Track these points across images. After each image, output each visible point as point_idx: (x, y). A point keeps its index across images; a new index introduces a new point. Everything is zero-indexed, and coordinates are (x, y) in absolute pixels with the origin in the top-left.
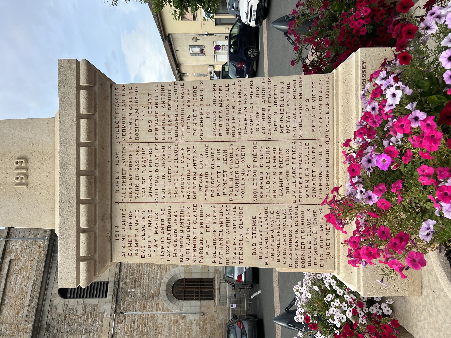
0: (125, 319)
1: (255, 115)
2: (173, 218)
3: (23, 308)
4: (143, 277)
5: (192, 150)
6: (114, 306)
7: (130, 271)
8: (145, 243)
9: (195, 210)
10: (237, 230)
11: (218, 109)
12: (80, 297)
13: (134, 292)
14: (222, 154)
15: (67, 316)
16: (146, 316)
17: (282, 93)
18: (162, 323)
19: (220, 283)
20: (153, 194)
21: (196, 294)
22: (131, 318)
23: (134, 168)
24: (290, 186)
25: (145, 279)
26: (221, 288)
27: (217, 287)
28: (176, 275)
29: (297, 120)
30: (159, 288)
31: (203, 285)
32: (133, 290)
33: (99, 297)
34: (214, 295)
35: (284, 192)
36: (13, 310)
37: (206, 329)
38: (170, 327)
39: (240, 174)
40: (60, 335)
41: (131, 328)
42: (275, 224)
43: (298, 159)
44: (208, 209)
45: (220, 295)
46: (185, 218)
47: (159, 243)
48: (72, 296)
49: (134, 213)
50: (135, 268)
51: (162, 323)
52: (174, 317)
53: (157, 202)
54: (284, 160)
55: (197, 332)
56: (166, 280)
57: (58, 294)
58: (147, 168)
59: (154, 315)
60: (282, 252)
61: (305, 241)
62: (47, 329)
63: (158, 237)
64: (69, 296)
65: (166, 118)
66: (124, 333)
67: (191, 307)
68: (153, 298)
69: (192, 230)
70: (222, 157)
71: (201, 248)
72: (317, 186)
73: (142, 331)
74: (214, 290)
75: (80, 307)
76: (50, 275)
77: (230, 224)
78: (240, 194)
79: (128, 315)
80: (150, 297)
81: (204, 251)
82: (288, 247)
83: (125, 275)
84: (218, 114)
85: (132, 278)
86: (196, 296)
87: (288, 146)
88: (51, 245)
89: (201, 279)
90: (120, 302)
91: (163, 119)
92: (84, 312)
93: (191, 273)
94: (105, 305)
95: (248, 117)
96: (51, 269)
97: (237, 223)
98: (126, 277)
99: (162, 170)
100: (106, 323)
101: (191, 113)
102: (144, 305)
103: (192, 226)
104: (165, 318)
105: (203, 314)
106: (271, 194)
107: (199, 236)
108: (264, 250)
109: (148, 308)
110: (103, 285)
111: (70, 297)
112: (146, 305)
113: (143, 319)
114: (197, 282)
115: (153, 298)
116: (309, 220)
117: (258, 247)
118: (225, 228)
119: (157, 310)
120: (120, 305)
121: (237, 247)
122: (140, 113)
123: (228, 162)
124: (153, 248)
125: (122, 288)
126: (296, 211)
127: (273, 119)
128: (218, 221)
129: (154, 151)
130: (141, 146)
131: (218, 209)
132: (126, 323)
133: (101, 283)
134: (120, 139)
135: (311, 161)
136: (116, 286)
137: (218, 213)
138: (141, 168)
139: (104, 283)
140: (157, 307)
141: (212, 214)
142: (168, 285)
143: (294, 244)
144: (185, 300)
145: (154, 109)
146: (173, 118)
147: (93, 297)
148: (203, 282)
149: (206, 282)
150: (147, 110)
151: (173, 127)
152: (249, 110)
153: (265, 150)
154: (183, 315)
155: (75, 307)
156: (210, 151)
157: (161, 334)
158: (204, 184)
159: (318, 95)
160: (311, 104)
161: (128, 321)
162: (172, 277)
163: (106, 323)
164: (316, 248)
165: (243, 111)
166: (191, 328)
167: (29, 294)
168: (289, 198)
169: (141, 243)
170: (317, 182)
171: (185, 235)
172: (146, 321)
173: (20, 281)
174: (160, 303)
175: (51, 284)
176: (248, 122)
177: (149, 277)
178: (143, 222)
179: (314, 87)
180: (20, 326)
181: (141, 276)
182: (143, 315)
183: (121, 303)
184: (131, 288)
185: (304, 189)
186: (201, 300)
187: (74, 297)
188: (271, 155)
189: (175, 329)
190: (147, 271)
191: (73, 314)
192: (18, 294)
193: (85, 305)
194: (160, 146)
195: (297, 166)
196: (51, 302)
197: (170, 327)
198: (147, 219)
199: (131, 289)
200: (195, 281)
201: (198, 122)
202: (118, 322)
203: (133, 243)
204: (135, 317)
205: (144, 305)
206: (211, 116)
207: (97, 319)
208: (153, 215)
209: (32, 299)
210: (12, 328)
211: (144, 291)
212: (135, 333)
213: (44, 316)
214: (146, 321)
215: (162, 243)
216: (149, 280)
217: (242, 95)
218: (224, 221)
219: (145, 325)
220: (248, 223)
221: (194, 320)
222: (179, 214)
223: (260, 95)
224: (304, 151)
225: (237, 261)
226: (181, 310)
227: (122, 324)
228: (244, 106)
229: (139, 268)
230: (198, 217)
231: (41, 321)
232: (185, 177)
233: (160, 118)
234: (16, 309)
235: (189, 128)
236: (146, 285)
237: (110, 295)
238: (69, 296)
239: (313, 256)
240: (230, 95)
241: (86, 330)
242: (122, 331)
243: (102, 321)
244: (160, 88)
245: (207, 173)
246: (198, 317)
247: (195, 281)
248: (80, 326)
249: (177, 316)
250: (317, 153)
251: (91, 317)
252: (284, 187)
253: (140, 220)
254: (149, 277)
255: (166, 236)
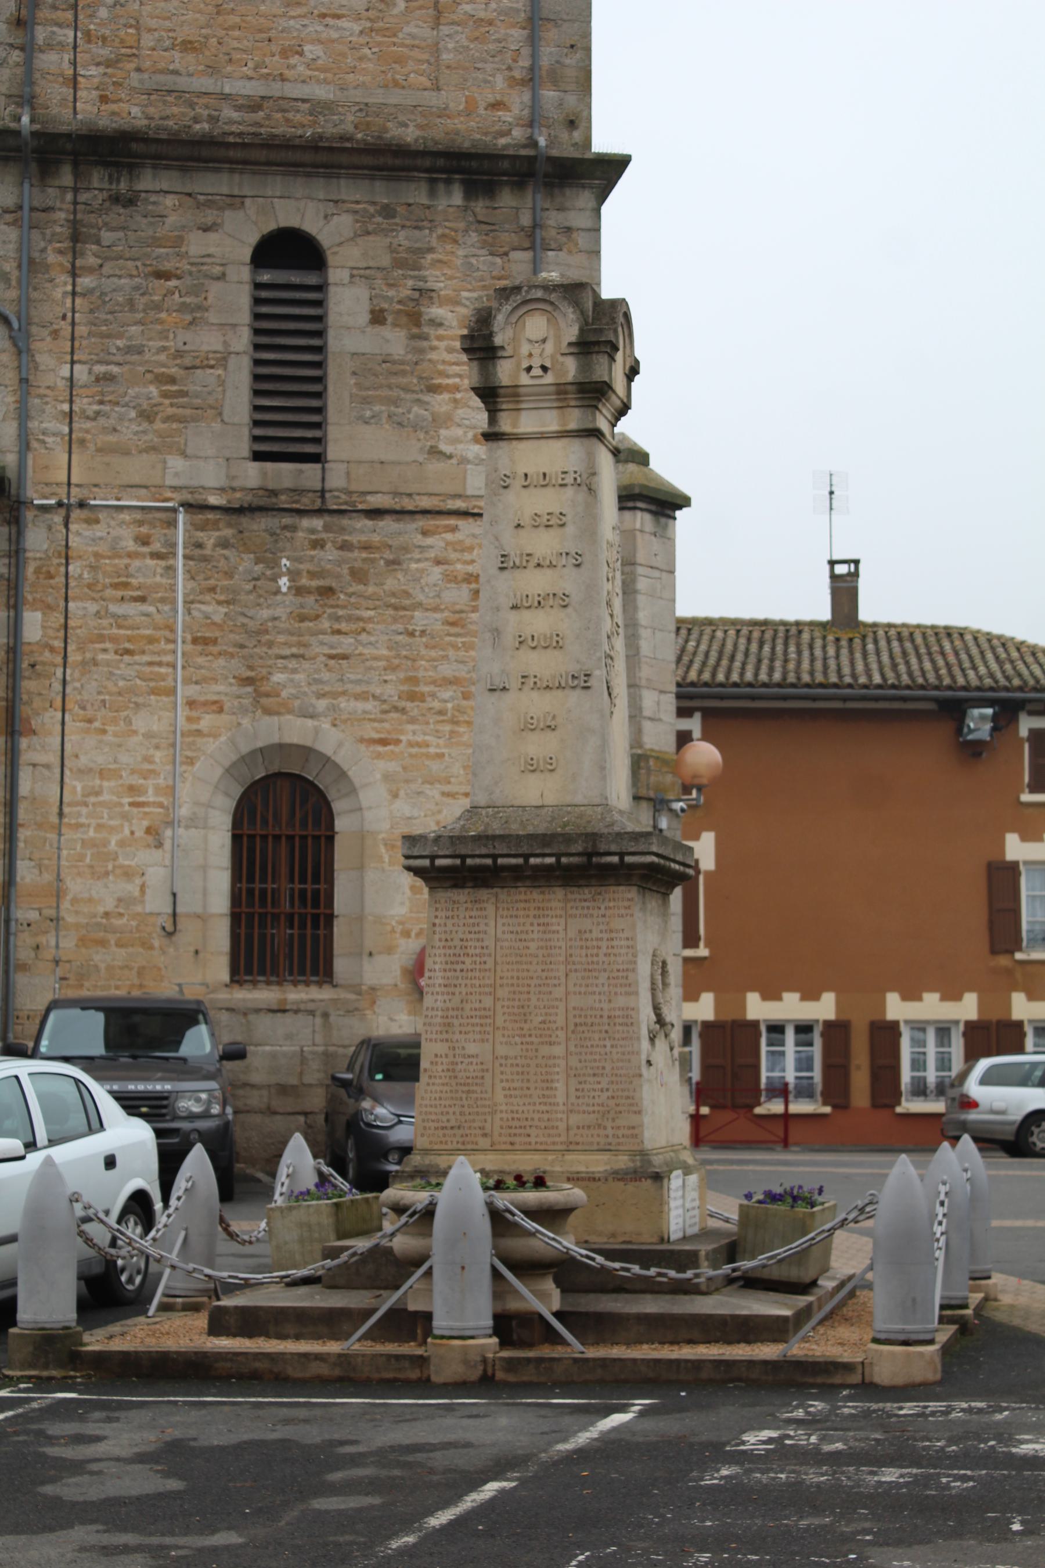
0: (156, 556)
1: (597, 1057)
2: (478, 959)
3: (212, 70)
4: (343, 626)
5: (556, 982)
6: (213, 500)
7: (373, 561)
8: (450, 927)
9: (488, 986)
10: (463, 1037)
11: (606, 1014)
12: (257, 332)
13: (278, 592)
14: (552, 1018)
15: (173, 283)
16: (165, 652)
17: (623, 1090)
18: (135, 732)
19: (312, 1013)
20: (506, 936)
21: (263, 892)
22: (159, 586)
23: (536, 912)
24: (513, 1100)
25: (336, 638)
26: (288, 1018)
27: (296, 995)
28: (353, 791)
29: (591, 1109)
30: (290, 712)
31: (303, 926)
32: (284, 582)
33: (256, 423)
34: (254, 983)
35: (507, 1092)
36: (202, 19)
37: (103, 943)
38: (116, 774)
39: (528, 1039)
40: (92, 261)
41: (116, 586)
42: (470, 1081)
43: (543, 1108)
44: (488, 1002)
45: (258, 1011)
46: (477, 974)
47: (450, 943)
48: (264, 294)
49: (484, 913)
50: (390, 584)
51: (135, 732)
52: (157, 789)
53: (497, 940)
54: (546, 1093)
55: (90, 900)
56: (330, 740)
57: (272, 226)
58: (536, 928)
59: (173, 692)
60: (438, 1088)
61: (451, 1117)
62: (115, 199)
63: (457, 942)
64: (266, 277)
65: (595, 951)
66: (97, 555)
67: (204, 871)
68: (249, 681)
69: (464, 982)
70: (549, 1018)
71: (443, 994)
72: (513, 1131)
73: (101, 639)
74: (279, 983)
75: (208, 341)
76: (364, 177)
77: (470, 1028)
78: (504, 1040)
79: (171, 570)
80: (251, 668)
81: (439, 997)
82: (443, 1095)
83: (354, 539)
84: (599, 1013)
85: (338, 576)
86: (250, 892)
87: (560, 1099)
88: (506, 165)
89: (330, 918)
90: (229, 525)
91: (593, 947)
92: (188, 361)
93: (361, 868)
94: (216, 458)
95: (594, 1050)
96: (388, 179)
97: (470, 1036)
98: (345, 546)
99: (533, 946)
100: (136, 468)
101: (601, 981)
102: (215, 641)
103: (469, 982)
104: (157, 747)
105: (170, 928)
106: (504, 1077)
107: (457, 990)
108: (440, 1068)
109: (200, 660)
110: (309, 434)
111: (258, 286)
112: (215, 649)
113: (151, 640)
114: (316, 893)
115: (249, 681)
116: (474, 1121)
117: (444, 1060)
118: (465, 1021)
119: (191, 704)
120: (215, 526)
121: (445, 1036)
122: (601, 920)
123: (542, 1026)
124: (443, 937)
125: (293, 528)
126: (484, 1106)
127: (591, 1079)
128: (473, 1013)
129: (556, 936)
130: (562, 921)
131: (487, 1013)
132: (137, 563)
133: (318, 426)
134: (570, 896)
135: (543, 1124)
136: (306, 502)
137: (483, 1013)
138: (535, 922)
139: (318, 441)
140: (205, 704)
141: (482, 1005)
142: (306, 752)
143: (447, 1103)
144: (236, 838)
145: (605, 936)
146: (595, 959)
147: (257, 393)
148: (316, 926)
149: (316, 939)
150: (603, 927)
151: (584, 959)
152: (603, 1051)
153: (557, 1069)
154: (168, 833)
155: (212, 317)
156: (556, 1003)
157: (87, 731)
158: (517, 997)
159: (620, 1133)
160: (609, 1124)
161: (146, 572)
162: (343, 775)
163: (136, 468)
164: (443, 1128)
165: (602, 1043)
166: (107, 873)
167: (276, 89)
168: (500, 1096)
169: (449, 922)
170: (518, 1131)
171: (458, 973)
172: (146, 658)
173: (335, 35)
174: (224, 717)
175: (319, 188)
176: (590, 1050)
177: (345, 657)
178: (474, 925)
179: (629, 1128)
180: (133, 66)
181: (349, 619)
182: (169, 641)
183: (228, 532)
184: (294, 575)
185: (510, 1116)
186: (235, 918)
187: (257, 301)
188: (549, 1077)
189: (106, 797)
190: (377, 643)
191: (183, 308)
192: (273, 34)
193: (223, 360)
194: (562, 944)
195: (538, 1107)
196: (235, 202)
197: (116, 774)
198: (476, 929)
199: (290, 572)
200: (322, 886)
201: (590, 989)
202: (140, 523)
203: (450, 913)
204: (163, 600)
205: (215, 641)
206: (597, 1005)
207: (159, 425)
208: (481, 936)
209: (255, 105)
210: (122, 33)
211: (281, 639)
212: (92, 607)
213: (175, 174)
214: (146, 658)
215: (450, 948)
216: (332, 657)
217: (621, 1042)
218: (474, 1021)
219: (128, 652)
220: (472, 1048)
221: (143, 888)
222: (483, 966)
223: (620, 1064)
224: (554, 1116)
225: (429, 1036)
226: (193, 822)
227: (130, 545)
228: (608, 1043)
229: (389, 606)
230: (478, 990)
231: (154, 167)
232: (525, 974)
233: (595, 943)
234: (206, 37)
235: (583, 978)
236: (305, 645)
237: (264, 474)
238: (266, 277)
239: (431, 1124)
240: (621, 1028)
241: (109, 378)
242: (102, 548)
243: (153, 449)
244: (630, 943)
245: (529, 1000)
246: (157, 903)
247: (322, 886)
248: (129, 350)
249: (161, 805)
250: (551, 1132)
251: (165, 395)
252: (512, 1092)
253: (476, 921)
254: (345, 657)
255: (458, 951)
